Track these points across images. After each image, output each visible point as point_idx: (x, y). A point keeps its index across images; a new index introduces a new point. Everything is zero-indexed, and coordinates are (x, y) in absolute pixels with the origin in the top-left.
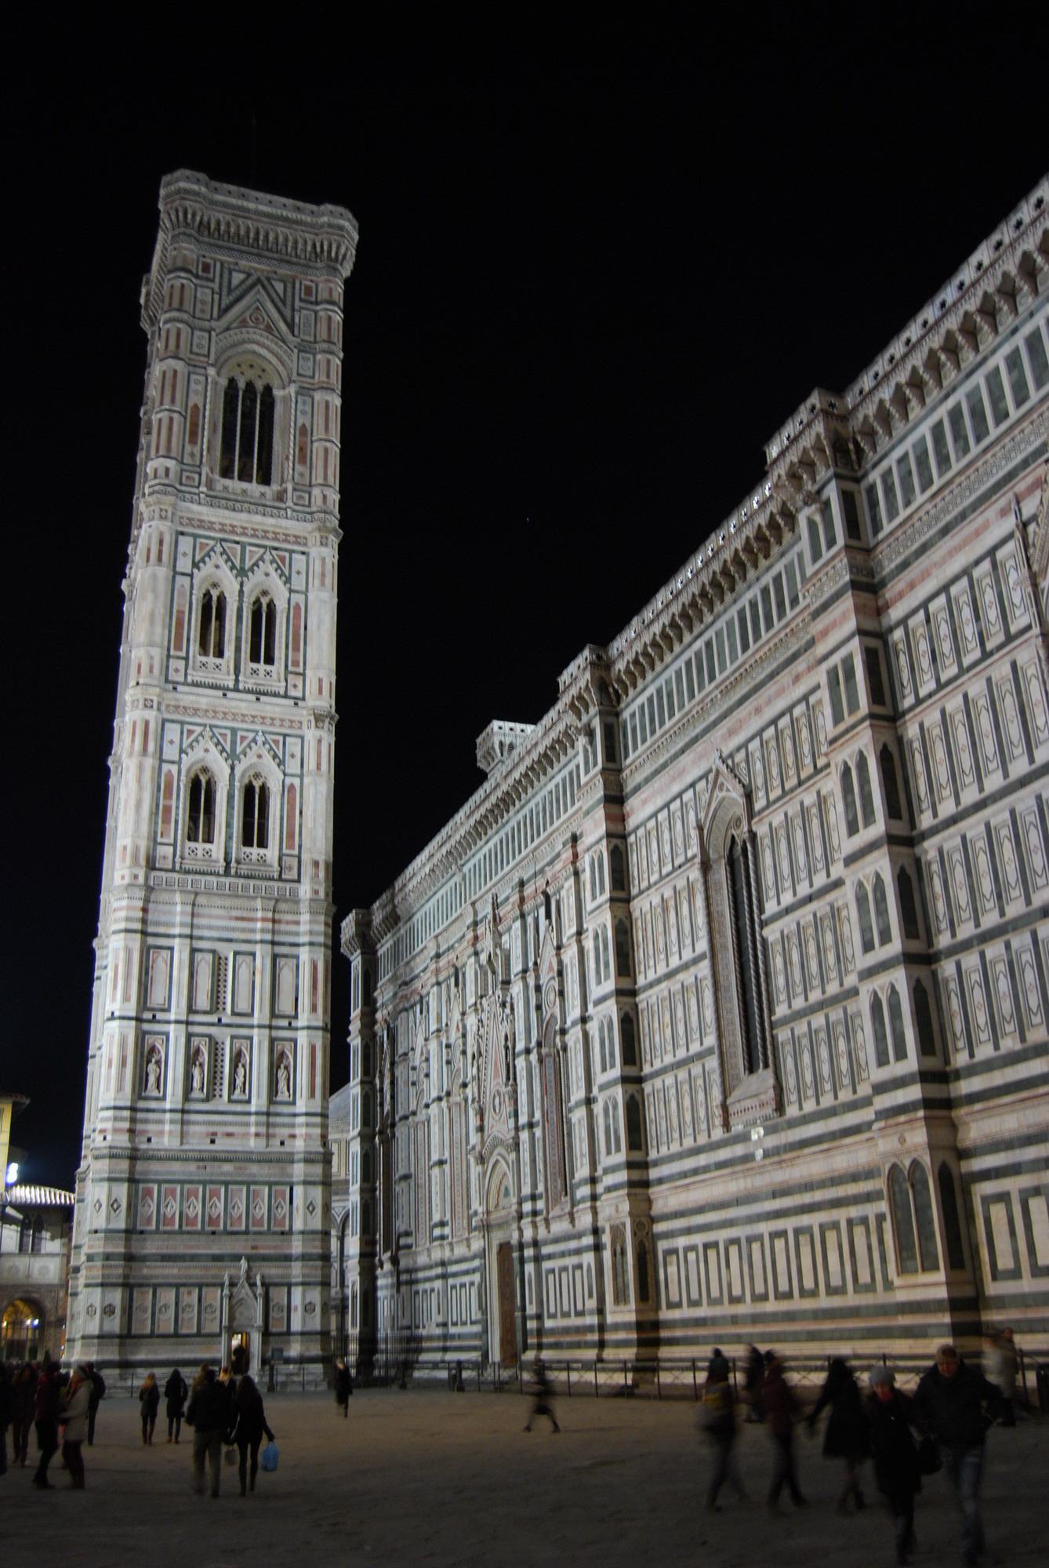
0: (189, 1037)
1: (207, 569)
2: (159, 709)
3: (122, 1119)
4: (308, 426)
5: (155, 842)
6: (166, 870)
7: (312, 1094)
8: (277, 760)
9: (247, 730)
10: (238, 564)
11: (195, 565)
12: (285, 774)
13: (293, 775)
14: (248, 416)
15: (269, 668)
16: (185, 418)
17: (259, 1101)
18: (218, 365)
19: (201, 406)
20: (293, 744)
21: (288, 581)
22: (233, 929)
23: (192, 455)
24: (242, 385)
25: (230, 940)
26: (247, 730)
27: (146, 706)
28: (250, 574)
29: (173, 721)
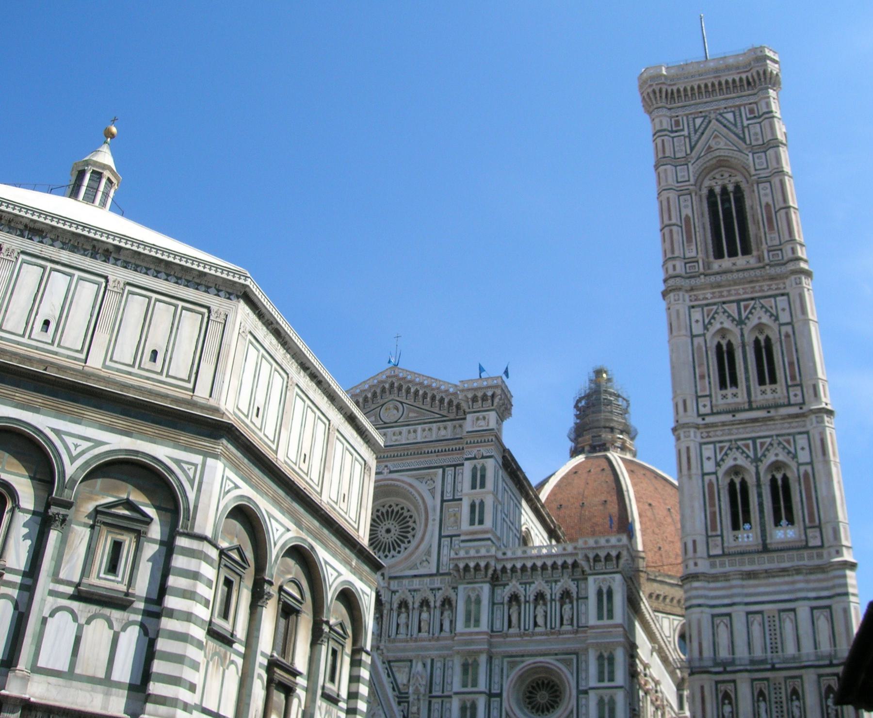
0: (753, 680)
2: (695, 437)
4: (771, 203)
5: (708, 537)
8: (791, 455)
10: (737, 318)
11: (706, 328)
14: (727, 213)
15: (773, 386)
16: (681, 227)
18: (698, 184)
19: (690, 215)
20: (802, 441)
21: (777, 319)
24: (718, 190)
27: (685, 437)
28: (747, 321)
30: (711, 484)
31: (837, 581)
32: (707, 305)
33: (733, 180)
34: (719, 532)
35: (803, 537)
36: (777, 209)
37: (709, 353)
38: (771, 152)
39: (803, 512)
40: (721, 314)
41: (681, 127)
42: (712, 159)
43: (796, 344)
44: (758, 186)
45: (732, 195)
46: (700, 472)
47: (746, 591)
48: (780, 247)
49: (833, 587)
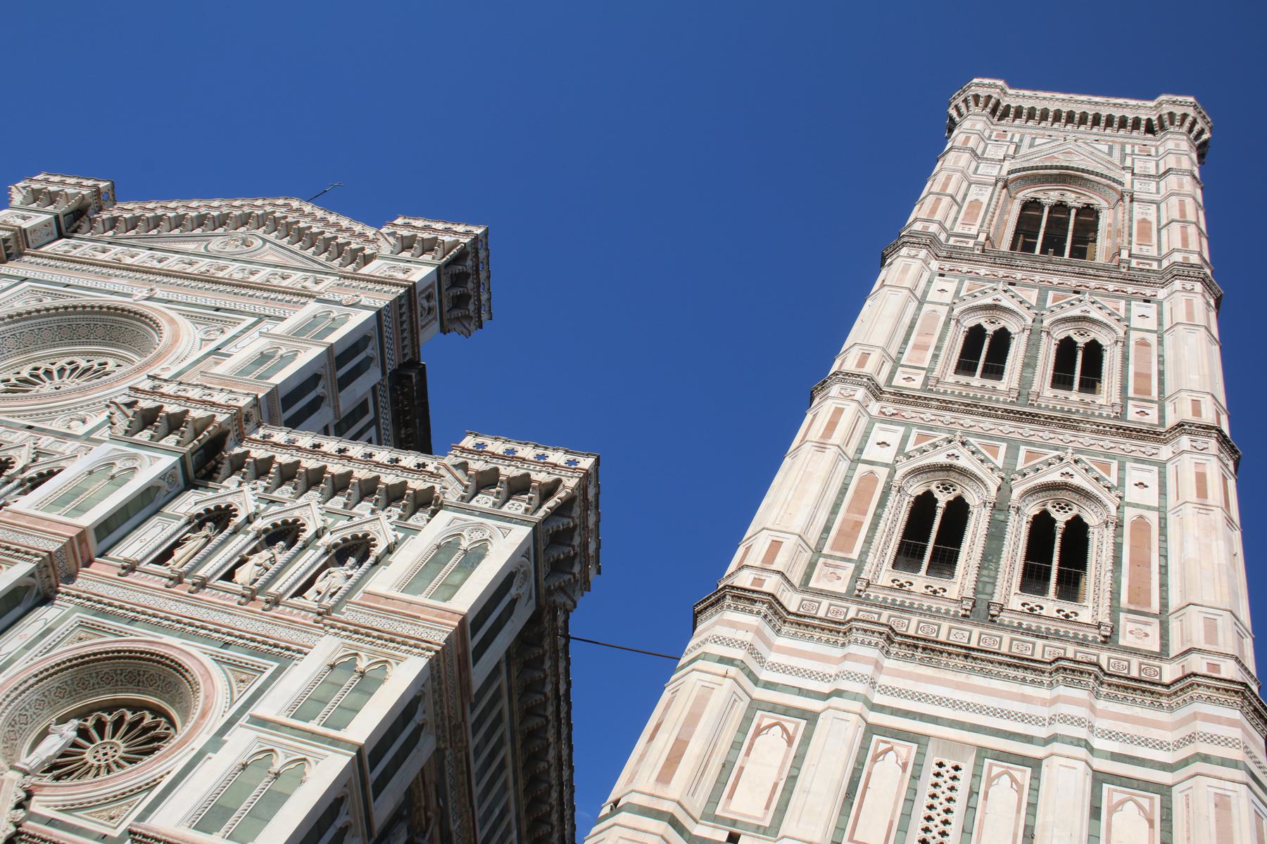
16: (960, 207)
26: (1041, 446)
30: (870, 479)
31: (1202, 727)
33: (1084, 200)
34: (855, 555)
35: (1107, 620)
36: (1164, 222)
37: (953, 322)
38: (1172, 179)
39: (1116, 582)
42: (1051, 168)
43: (1160, 356)
44: (1132, 201)
45: (1073, 212)
46: (851, 451)
47: (883, 680)
48: (1159, 257)
49: (1191, 738)
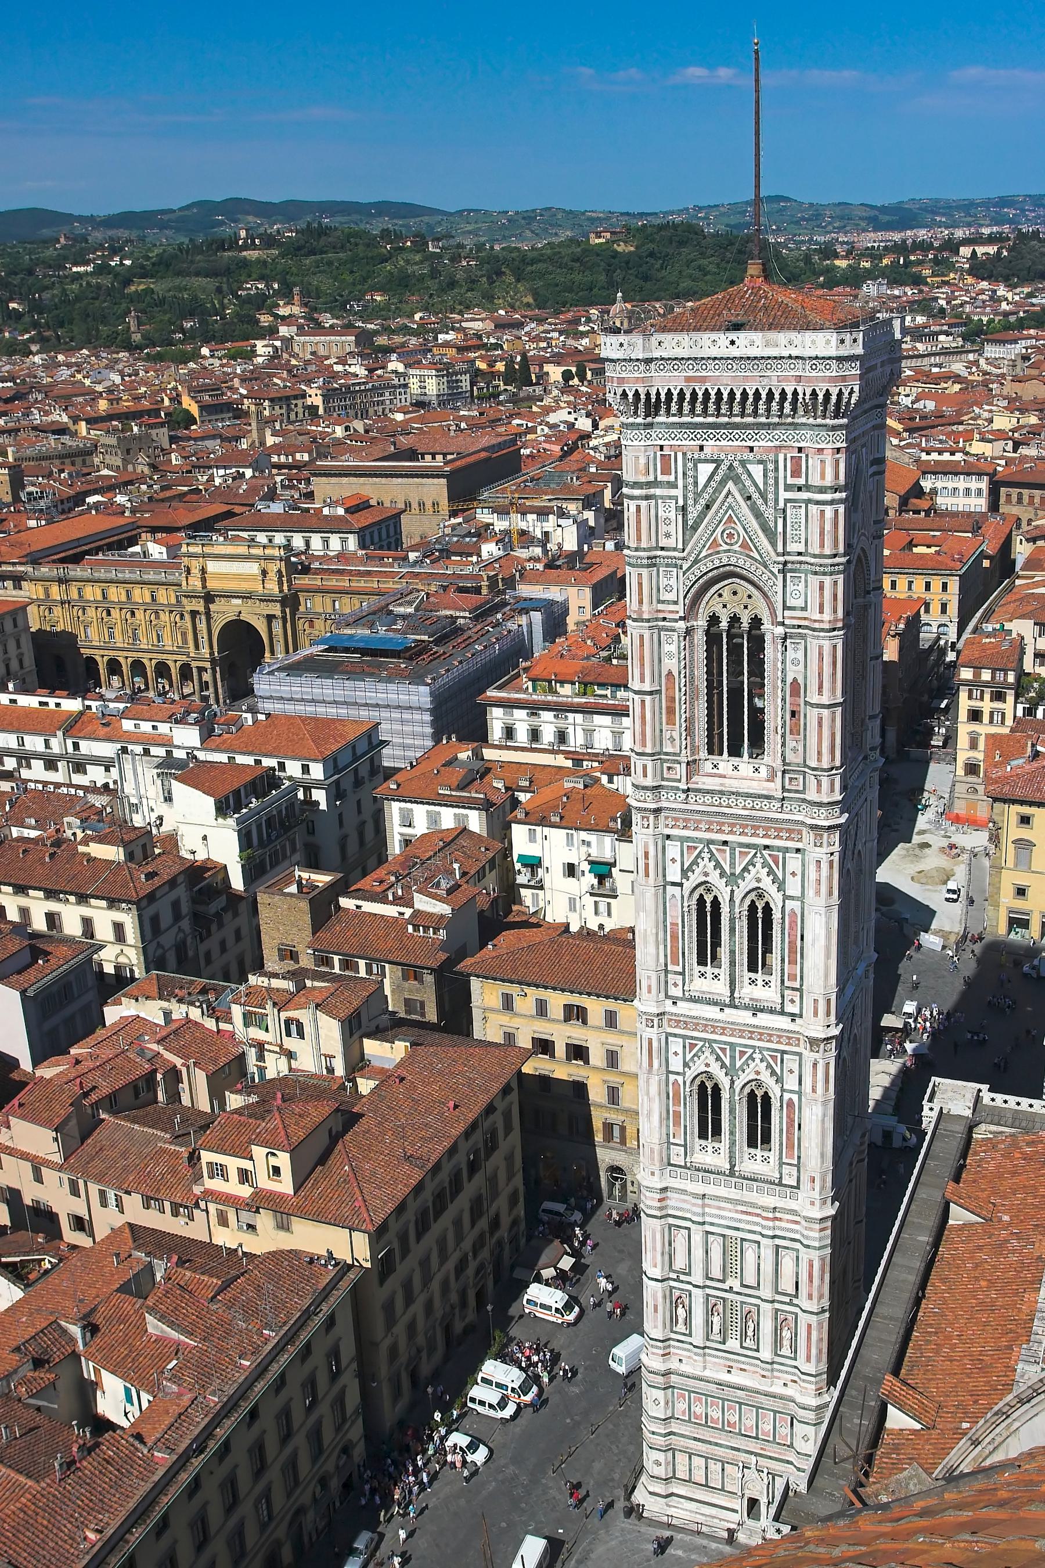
1: (695, 878)
3: (657, 1347)
4: (801, 681)
5: (669, 1143)
6: (680, 1166)
7: (808, 1359)
9: (746, 1046)
12: (783, 1090)
13: (791, 1092)
17: (766, 1354)
19: (676, 674)
20: (791, 1062)
22: (740, 1221)
23: (672, 739)
25: (737, 1229)
29: (675, 1035)
32: (688, 839)
40: (706, 860)
41: (672, 478)
47: (707, 1210)
